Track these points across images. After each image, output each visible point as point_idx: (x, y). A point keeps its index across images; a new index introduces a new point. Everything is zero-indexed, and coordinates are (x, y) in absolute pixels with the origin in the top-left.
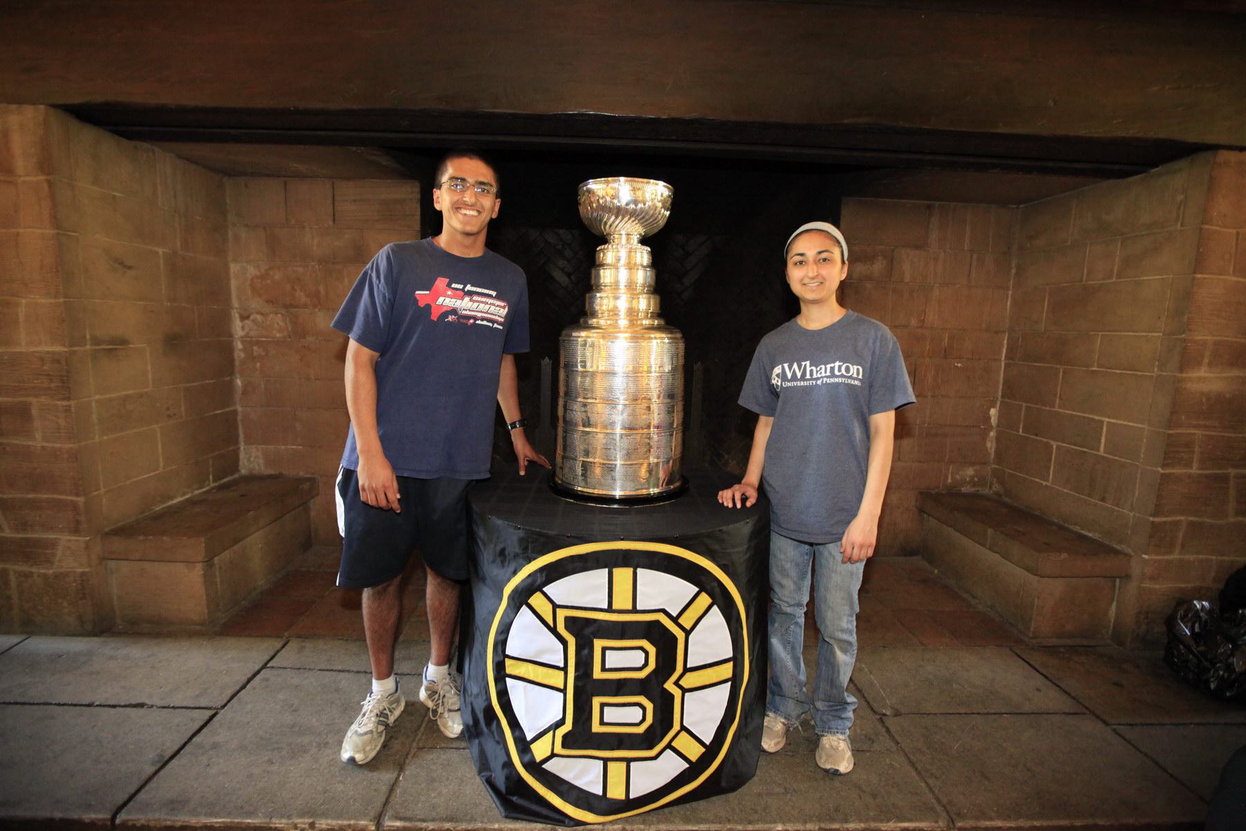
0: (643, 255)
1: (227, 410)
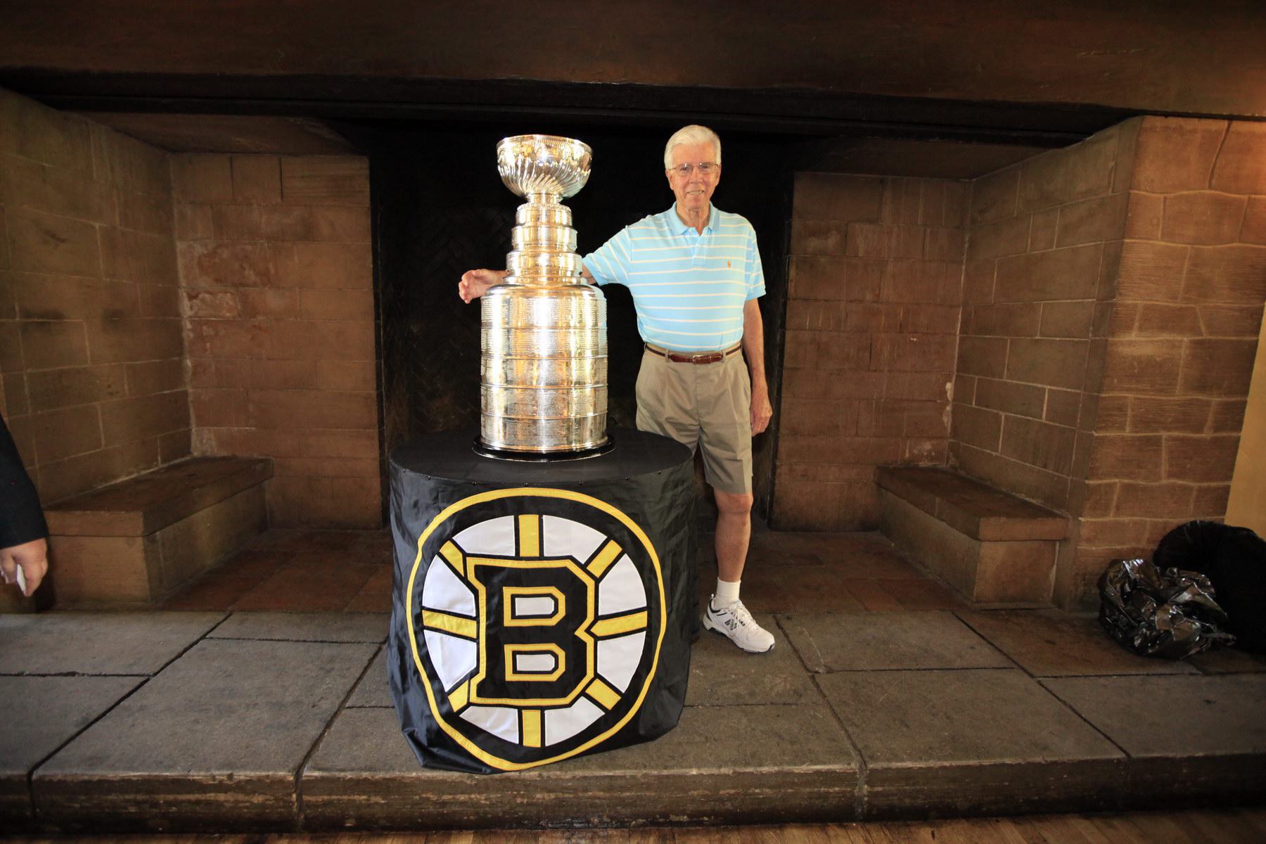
0: (564, 215)
1: (176, 390)
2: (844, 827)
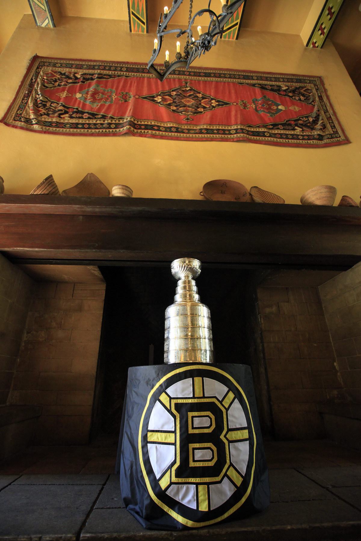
0: (193, 283)
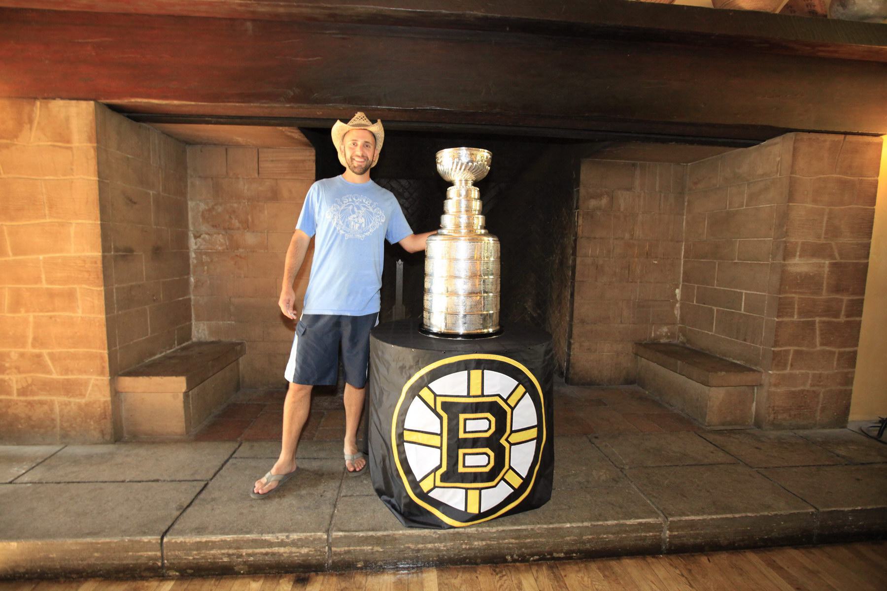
0: (475, 193)
1: (185, 297)
2: (657, 558)
